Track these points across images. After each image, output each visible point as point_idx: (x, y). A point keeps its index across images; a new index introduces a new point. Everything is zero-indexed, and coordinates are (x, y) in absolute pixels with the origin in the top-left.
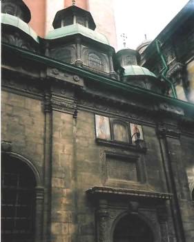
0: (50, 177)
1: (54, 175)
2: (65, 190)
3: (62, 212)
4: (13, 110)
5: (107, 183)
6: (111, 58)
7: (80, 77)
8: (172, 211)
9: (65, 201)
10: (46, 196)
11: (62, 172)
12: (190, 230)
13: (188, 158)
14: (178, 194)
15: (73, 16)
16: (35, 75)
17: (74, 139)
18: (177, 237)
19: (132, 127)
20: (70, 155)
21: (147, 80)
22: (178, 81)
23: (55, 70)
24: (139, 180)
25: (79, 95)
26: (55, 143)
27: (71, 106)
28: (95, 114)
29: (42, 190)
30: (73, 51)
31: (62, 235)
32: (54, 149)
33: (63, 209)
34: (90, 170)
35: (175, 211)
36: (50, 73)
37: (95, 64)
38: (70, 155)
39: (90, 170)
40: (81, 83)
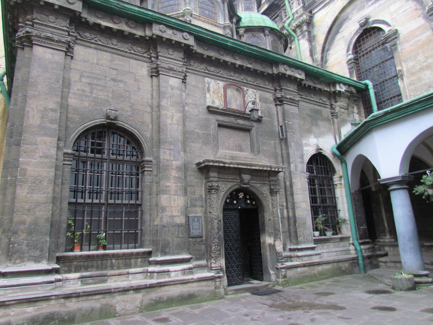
0: (159, 147)
1: (161, 147)
2: (174, 163)
5: (218, 154)
6: (226, 4)
7: (190, 33)
9: (174, 173)
10: (154, 168)
11: (170, 143)
12: (300, 202)
13: (306, 127)
14: (292, 165)
16: (139, 33)
17: (184, 107)
18: (287, 208)
21: (267, 32)
23: (162, 27)
24: (252, 151)
26: (163, 112)
27: (180, 70)
29: (151, 162)
31: (172, 207)
33: (172, 181)
34: (200, 141)
35: (288, 183)
37: (207, 12)
39: (200, 141)
40: (191, 41)
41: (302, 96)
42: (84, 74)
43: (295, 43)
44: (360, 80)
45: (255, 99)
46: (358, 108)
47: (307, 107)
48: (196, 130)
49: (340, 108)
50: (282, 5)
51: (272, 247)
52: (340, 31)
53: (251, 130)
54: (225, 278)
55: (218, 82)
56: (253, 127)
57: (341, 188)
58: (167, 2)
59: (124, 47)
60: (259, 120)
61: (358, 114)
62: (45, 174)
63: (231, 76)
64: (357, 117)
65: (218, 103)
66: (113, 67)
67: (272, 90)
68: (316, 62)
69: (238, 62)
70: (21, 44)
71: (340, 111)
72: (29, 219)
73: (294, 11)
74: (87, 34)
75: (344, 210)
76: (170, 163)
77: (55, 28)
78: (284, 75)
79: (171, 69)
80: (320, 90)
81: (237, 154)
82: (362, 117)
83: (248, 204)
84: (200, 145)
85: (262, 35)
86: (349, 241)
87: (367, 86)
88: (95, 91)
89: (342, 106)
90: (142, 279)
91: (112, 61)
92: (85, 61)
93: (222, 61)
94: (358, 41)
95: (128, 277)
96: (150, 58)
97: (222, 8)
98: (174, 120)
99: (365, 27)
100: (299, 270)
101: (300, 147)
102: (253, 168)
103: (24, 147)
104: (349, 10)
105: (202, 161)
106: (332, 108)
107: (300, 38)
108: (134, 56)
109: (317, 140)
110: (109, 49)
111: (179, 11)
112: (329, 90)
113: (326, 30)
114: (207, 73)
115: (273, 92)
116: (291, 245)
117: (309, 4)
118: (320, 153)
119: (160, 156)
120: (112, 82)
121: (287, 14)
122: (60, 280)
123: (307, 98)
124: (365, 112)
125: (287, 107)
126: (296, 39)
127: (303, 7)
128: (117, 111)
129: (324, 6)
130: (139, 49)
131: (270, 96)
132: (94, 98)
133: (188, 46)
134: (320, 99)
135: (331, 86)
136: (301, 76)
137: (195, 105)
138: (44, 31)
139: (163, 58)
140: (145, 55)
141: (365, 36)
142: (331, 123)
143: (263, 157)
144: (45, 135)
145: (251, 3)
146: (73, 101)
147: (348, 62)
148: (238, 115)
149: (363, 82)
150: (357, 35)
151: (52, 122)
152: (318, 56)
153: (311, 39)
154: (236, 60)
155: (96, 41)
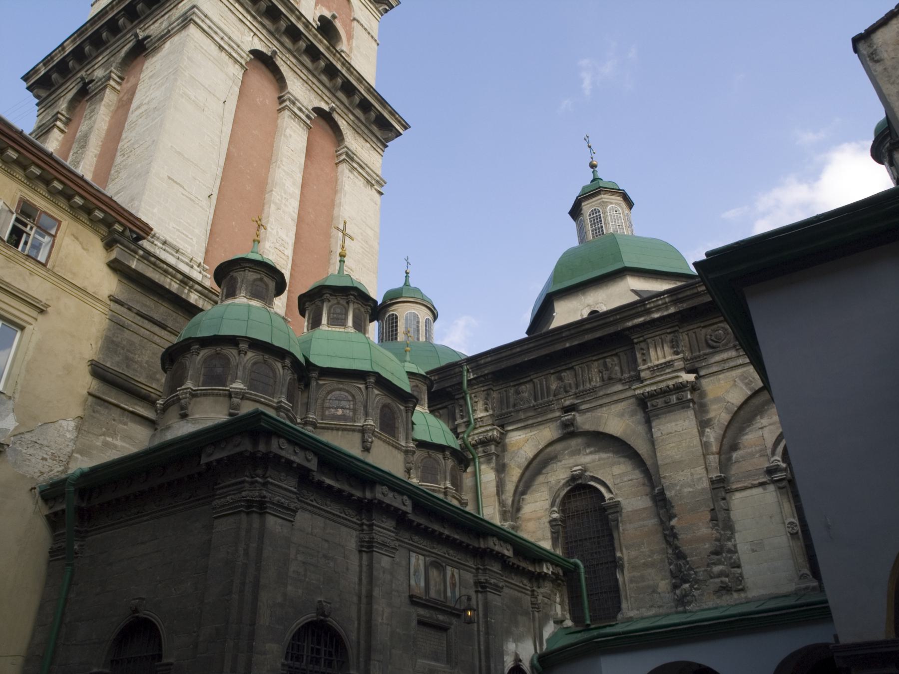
0: (368, 660)
5: (417, 666)
7: (410, 497)
15: (348, 303)
16: (358, 494)
19: (449, 569)
20: (388, 625)
22: (488, 456)
23: (385, 488)
25: (401, 520)
26: (375, 607)
27: (392, 544)
28: (410, 550)
30: (359, 398)
36: (379, 496)
38: (388, 625)
41: (502, 576)
43: (475, 465)
44: (568, 558)
46: (561, 596)
48: (398, 630)
49: (543, 597)
50: (457, 397)
52: (544, 471)
53: (449, 629)
58: (337, 401)
59: (334, 508)
61: (560, 604)
63: (434, 548)
64: (558, 608)
67: (474, 568)
70: (248, 507)
71: (543, 601)
73: (480, 414)
74: (305, 492)
77: (286, 489)
78: (492, 550)
79: (384, 545)
80: (524, 569)
82: (565, 611)
85: (440, 456)
87: (576, 565)
89: (545, 595)
93: (430, 529)
94: (568, 496)
96: (362, 524)
98: (384, 617)
99: (580, 481)
101: (501, 654)
104: (558, 447)
106: (533, 595)
107: (482, 460)
108: (345, 521)
109: (517, 645)
111: (355, 422)
112: (533, 570)
113: (524, 462)
114: (411, 545)
115: (474, 571)
118: (520, 665)
121: (464, 414)
123: (507, 579)
124: (569, 603)
125: (490, 596)
128: (330, 603)
131: (469, 577)
133: (405, 513)
134: (522, 582)
135: (537, 565)
136: (508, 552)
139: (377, 528)
140: (354, 520)
141: (577, 493)
142: (530, 618)
145: (421, 393)
146: (289, 588)
147: (550, 522)
148: (440, 607)
149: (572, 560)
150: (567, 487)
152: (508, 497)
153: (501, 469)
154: (444, 528)
155: (312, 501)
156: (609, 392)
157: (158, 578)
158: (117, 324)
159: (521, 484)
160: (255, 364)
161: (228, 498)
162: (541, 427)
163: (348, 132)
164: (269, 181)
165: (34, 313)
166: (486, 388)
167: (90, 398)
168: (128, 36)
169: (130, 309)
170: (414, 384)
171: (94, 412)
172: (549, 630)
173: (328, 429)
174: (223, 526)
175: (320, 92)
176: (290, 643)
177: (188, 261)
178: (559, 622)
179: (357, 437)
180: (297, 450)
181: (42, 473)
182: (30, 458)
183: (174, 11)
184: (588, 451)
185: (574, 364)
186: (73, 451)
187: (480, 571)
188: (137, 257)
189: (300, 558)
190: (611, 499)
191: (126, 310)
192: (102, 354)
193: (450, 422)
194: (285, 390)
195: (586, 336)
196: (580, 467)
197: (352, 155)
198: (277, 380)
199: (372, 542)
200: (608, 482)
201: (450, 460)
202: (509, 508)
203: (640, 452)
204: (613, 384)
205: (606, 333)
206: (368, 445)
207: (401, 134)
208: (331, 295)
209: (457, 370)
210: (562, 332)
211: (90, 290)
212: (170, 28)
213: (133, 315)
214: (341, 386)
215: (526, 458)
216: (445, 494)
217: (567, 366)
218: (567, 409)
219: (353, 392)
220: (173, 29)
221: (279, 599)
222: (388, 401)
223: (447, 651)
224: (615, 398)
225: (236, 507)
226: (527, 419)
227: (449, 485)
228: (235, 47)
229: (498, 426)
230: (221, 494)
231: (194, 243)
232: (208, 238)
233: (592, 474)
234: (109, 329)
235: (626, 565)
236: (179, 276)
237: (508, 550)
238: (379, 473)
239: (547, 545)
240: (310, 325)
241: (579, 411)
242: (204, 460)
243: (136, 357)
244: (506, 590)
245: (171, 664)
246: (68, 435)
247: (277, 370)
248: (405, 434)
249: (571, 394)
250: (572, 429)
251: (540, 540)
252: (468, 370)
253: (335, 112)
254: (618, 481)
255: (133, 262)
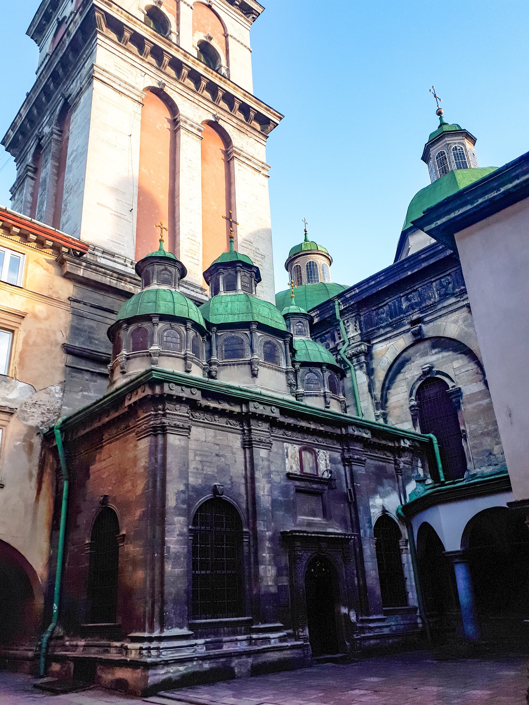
1: (258, 519)
2: (267, 533)
3: (266, 555)
4: (220, 449)
5: (298, 522)
7: (276, 407)
8: (355, 550)
9: (268, 544)
10: (251, 539)
11: (264, 513)
12: (370, 570)
14: (362, 531)
15: (236, 272)
16: (236, 409)
25: (273, 423)
26: (257, 484)
30: (246, 341)
31: (267, 577)
32: (257, 490)
33: (267, 552)
36: (252, 409)
38: (269, 495)
39: (283, 508)
42: (197, 452)
45: (326, 460)
46: (422, 462)
47: (371, 464)
48: (280, 498)
50: (335, 324)
51: (347, 616)
54: (310, 647)
55: (295, 445)
56: (325, 490)
57: (407, 553)
59: (222, 421)
60: (329, 482)
62: (181, 550)
64: (421, 471)
65: (295, 469)
66: (217, 443)
68: (375, 399)
69: (313, 426)
71: (404, 467)
72: (173, 590)
73: (351, 335)
74: (197, 414)
75: (410, 578)
76: (263, 534)
77: (180, 416)
79: (261, 441)
81: (312, 520)
83: (324, 572)
84: (283, 513)
86: (416, 613)
87: (431, 439)
88: (205, 468)
90: (247, 646)
91: (215, 437)
92: (197, 440)
95: (237, 644)
97: (284, 350)
98: (265, 491)
100: (372, 642)
101: (367, 509)
102: (330, 536)
103: (167, 528)
104: (411, 351)
105: (288, 531)
106: (396, 463)
107: (356, 367)
110: (213, 426)
112: (393, 445)
116: (362, 616)
117: (369, 332)
119: (256, 527)
120: (216, 458)
122: (196, 645)
123: (372, 454)
124: (429, 466)
126: (352, 369)
127: (361, 334)
129: (385, 340)
130: (234, 422)
131: (337, 456)
132: (205, 474)
133: (275, 418)
134: (385, 454)
136: (367, 435)
137: (277, 472)
138: (173, 419)
140: (238, 427)
143: (335, 523)
144: (180, 515)
147: (410, 408)
149: (427, 435)
150: (420, 381)
151: (184, 502)
152: (378, 393)
153: (370, 372)
155: (204, 420)
156: (445, 305)
157: (114, 482)
158: (77, 315)
159: (387, 382)
160: (165, 330)
161: (143, 427)
162: (397, 338)
163: (233, 133)
164: (176, 188)
165: (18, 320)
166: (354, 314)
167: (68, 368)
168: (59, 97)
169: (85, 304)
170: (298, 321)
171: (72, 377)
172: (411, 487)
173: (227, 365)
174: (144, 444)
175: (206, 107)
176: (196, 516)
177: (123, 262)
178: (421, 481)
179: (247, 368)
180: (184, 388)
181: (43, 422)
182: (33, 414)
183: (83, 70)
184: (434, 352)
185: (417, 287)
186: (62, 405)
187: (346, 450)
188: (82, 267)
189: (198, 458)
190: (453, 387)
191: (82, 305)
192: (72, 338)
193: (333, 343)
194: (190, 344)
195: (423, 264)
196: (428, 365)
197: (239, 152)
198: (183, 339)
199: (251, 441)
200: (450, 374)
201: (327, 372)
202: (379, 400)
203: (472, 349)
204: (448, 299)
205: (438, 259)
206: (256, 372)
207: (277, 124)
208: (224, 269)
209: (332, 304)
210: (404, 265)
211: (54, 296)
212: (81, 86)
213: (89, 307)
214: (233, 334)
215: (388, 363)
216: (325, 397)
217: (413, 289)
218: (413, 323)
219: (242, 337)
220: (83, 86)
221: (182, 488)
222: (269, 339)
223: (323, 509)
224: (451, 309)
225: (147, 432)
226: (386, 333)
227: (327, 390)
228: (131, 89)
229: (365, 342)
230: (140, 424)
231: (126, 248)
232: (135, 241)
233: (438, 369)
234: (72, 321)
235: (469, 435)
236: (115, 275)
237: (367, 434)
238: (249, 394)
239: (407, 426)
240: (213, 293)
241: (425, 323)
242: (127, 404)
243: (96, 336)
244: (368, 461)
245: (124, 535)
246: (57, 395)
247: (182, 333)
248: (285, 360)
249: (416, 310)
250: (419, 337)
251: (402, 422)
252: (339, 304)
253: (220, 120)
254: (457, 373)
255: (80, 271)
